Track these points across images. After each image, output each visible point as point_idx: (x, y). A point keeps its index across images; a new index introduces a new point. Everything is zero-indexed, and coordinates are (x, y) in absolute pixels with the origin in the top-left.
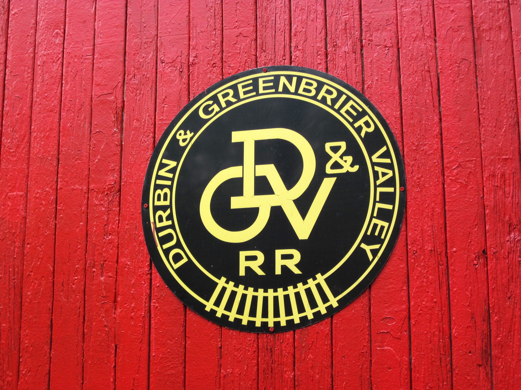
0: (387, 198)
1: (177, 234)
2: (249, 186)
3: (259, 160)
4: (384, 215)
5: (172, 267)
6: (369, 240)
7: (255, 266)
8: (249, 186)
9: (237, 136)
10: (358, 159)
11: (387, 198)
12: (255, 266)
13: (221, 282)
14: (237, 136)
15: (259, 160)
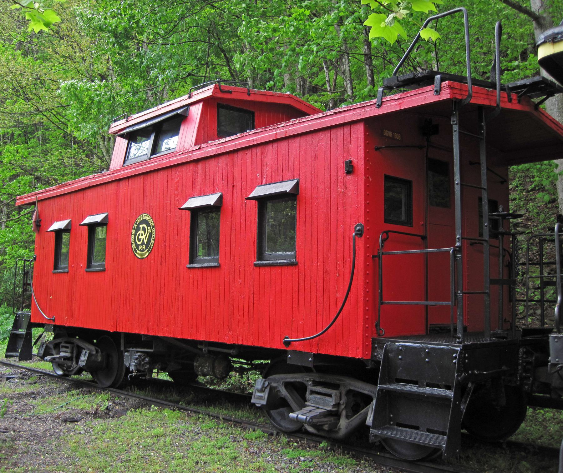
4: (153, 240)
5: (133, 248)
6: (152, 244)
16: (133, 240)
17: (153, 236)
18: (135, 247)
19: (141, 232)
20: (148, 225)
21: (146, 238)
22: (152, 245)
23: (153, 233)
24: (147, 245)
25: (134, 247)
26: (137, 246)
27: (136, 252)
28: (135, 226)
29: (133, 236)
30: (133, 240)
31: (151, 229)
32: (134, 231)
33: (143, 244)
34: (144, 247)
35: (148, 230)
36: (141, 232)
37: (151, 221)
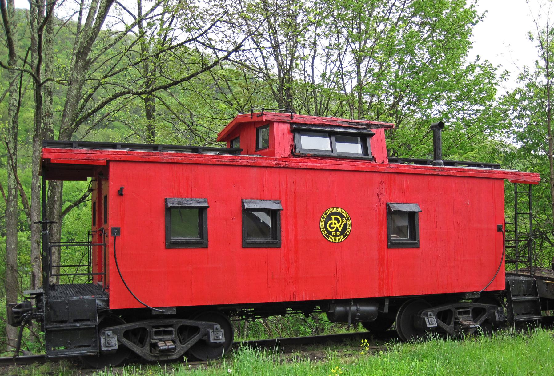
0: (350, 226)
1: (324, 230)
2: (333, 223)
3: (335, 220)
4: (349, 228)
5: (324, 234)
6: (348, 231)
7: (335, 234)
8: (333, 223)
9: (332, 216)
10: (346, 221)
11: (350, 226)
12: (335, 234)
13: (330, 236)
14: (332, 216)
15: (335, 220)
16: (322, 228)
17: (348, 225)
18: (326, 233)
19: (333, 221)
20: (342, 216)
21: (340, 226)
22: (348, 233)
23: (349, 222)
24: (342, 232)
25: (324, 233)
26: (330, 233)
27: (328, 237)
28: (325, 216)
29: (322, 224)
30: (322, 228)
31: (346, 220)
32: (323, 221)
33: (337, 229)
34: (338, 234)
35: (342, 220)
36: (333, 221)
37: (345, 214)
